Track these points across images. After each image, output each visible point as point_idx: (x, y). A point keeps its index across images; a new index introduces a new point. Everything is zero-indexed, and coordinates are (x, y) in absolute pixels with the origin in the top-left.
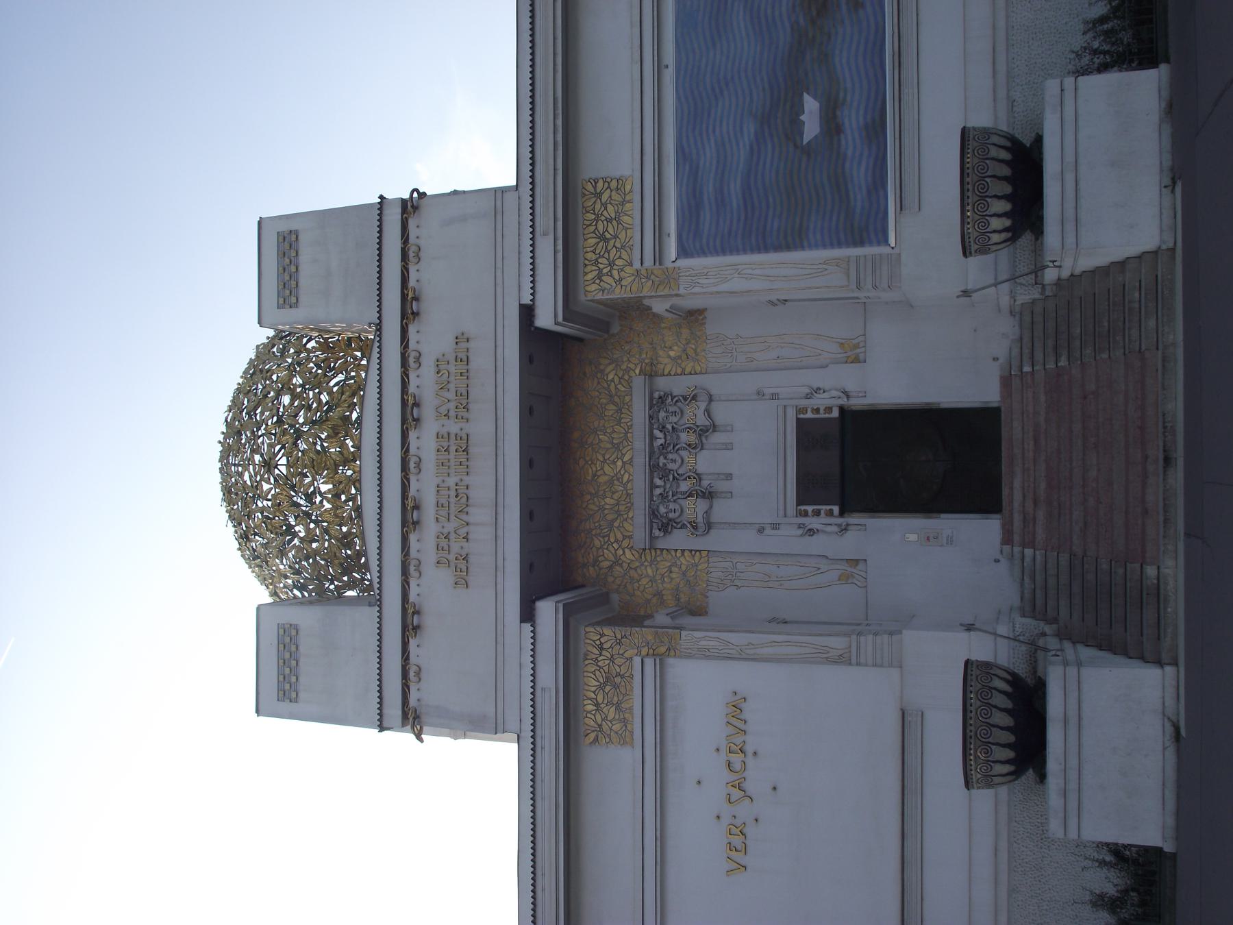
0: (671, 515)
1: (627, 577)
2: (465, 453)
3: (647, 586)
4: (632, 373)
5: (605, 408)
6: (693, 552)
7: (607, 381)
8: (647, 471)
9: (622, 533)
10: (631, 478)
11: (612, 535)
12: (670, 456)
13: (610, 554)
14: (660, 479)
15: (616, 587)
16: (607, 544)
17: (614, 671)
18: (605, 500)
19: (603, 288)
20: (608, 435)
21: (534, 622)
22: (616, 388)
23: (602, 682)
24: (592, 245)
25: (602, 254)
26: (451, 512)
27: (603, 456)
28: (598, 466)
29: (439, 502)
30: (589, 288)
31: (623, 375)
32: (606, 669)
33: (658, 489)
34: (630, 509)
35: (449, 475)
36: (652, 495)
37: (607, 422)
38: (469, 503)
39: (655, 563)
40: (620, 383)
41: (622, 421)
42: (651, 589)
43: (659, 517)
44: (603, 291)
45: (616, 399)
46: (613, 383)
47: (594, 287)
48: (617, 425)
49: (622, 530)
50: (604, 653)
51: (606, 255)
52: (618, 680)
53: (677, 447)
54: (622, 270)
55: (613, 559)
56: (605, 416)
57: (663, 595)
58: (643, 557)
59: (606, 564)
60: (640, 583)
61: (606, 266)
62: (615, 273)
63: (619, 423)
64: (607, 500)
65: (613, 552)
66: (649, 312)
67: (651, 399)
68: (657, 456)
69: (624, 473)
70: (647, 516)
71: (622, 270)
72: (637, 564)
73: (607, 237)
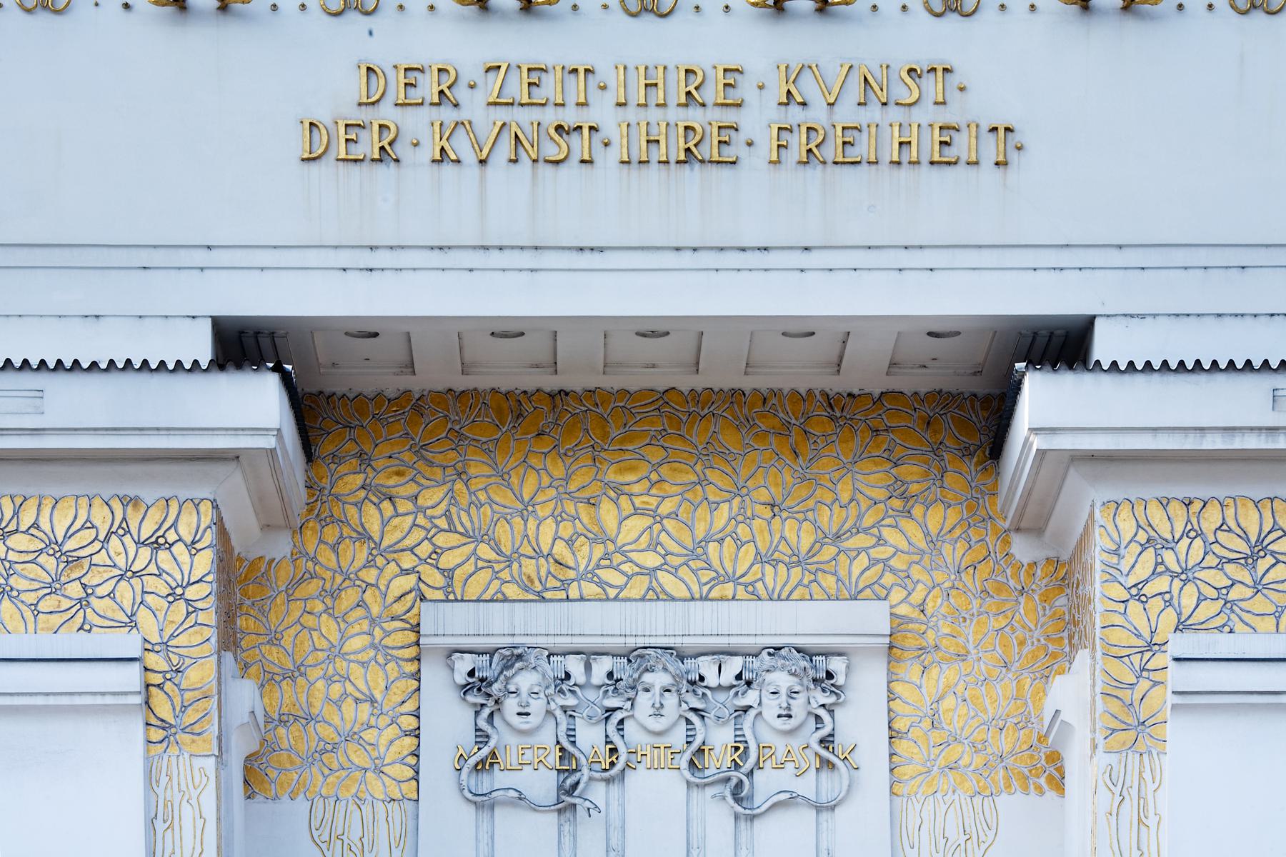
0: (511, 705)
1: (339, 579)
2: (682, 157)
3: (315, 634)
4: (897, 595)
5: (806, 520)
7: (878, 524)
9: (459, 565)
10: (612, 593)
11: (454, 539)
12: (671, 700)
13: (398, 535)
15: (311, 549)
16: (429, 526)
17: (95, 582)
18: (550, 520)
19: (1122, 551)
20: (729, 529)
21: (222, 367)
22: (859, 551)
24: (1241, 521)
25: (1216, 548)
26: (516, 109)
27: (674, 515)
28: (645, 498)
29: (544, 75)
30: (1125, 512)
31: (894, 571)
32: (101, 558)
34: (527, 589)
35: (619, 105)
37: (764, 523)
38: (541, 164)
40: (873, 562)
41: (768, 569)
42: (307, 646)
44: (1116, 552)
45: (830, 551)
46: (874, 540)
47: (1127, 526)
48: (758, 553)
49: (469, 567)
50: (145, 553)
51: (1211, 560)
52: (75, 590)
54: (1169, 603)
55: (385, 544)
56: (784, 521)
59: (373, 524)
60: (324, 616)
61: (1182, 558)
62: (1162, 584)
63: (760, 559)
64: (548, 529)
65: (408, 542)
66: (1066, 641)
67: (828, 654)
68: (671, 668)
69: (623, 573)
71: (1169, 603)
72: (375, 610)
73: (1260, 561)
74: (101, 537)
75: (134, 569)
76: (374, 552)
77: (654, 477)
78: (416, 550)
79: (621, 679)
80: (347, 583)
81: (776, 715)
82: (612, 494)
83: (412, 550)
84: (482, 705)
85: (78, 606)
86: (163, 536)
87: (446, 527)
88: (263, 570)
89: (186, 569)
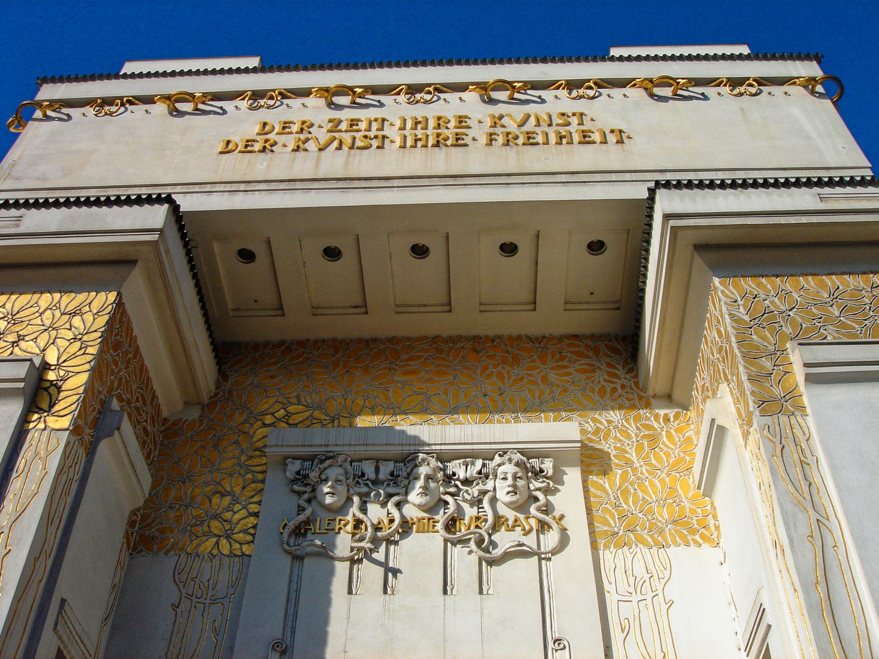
6: (252, 532)
8: (407, 448)
13: (266, 406)
14: (392, 474)
16: (285, 401)
23: (14, 318)
32: (38, 321)
33: (373, 469)
36: (360, 461)
39: (242, 472)
43: (322, 466)
49: (308, 423)
53: (448, 498)
57: (184, 483)
58: (257, 453)
65: (271, 410)
67: (541, 455)
70: (325, 449)
74: (41, 311)
75: (54, 326)
76: (250, 416)
77: (427, 377)
78: (276, 415)
79: (399, 476)
80: (230, 432)
81: (506, 493)
82: (399, 385)
83: (273, 414)
84: (305, 492)
85: (11, 346)
86: (80, 310)
87: (296, 403)
88: (180, 425)
89: (88, 325)
